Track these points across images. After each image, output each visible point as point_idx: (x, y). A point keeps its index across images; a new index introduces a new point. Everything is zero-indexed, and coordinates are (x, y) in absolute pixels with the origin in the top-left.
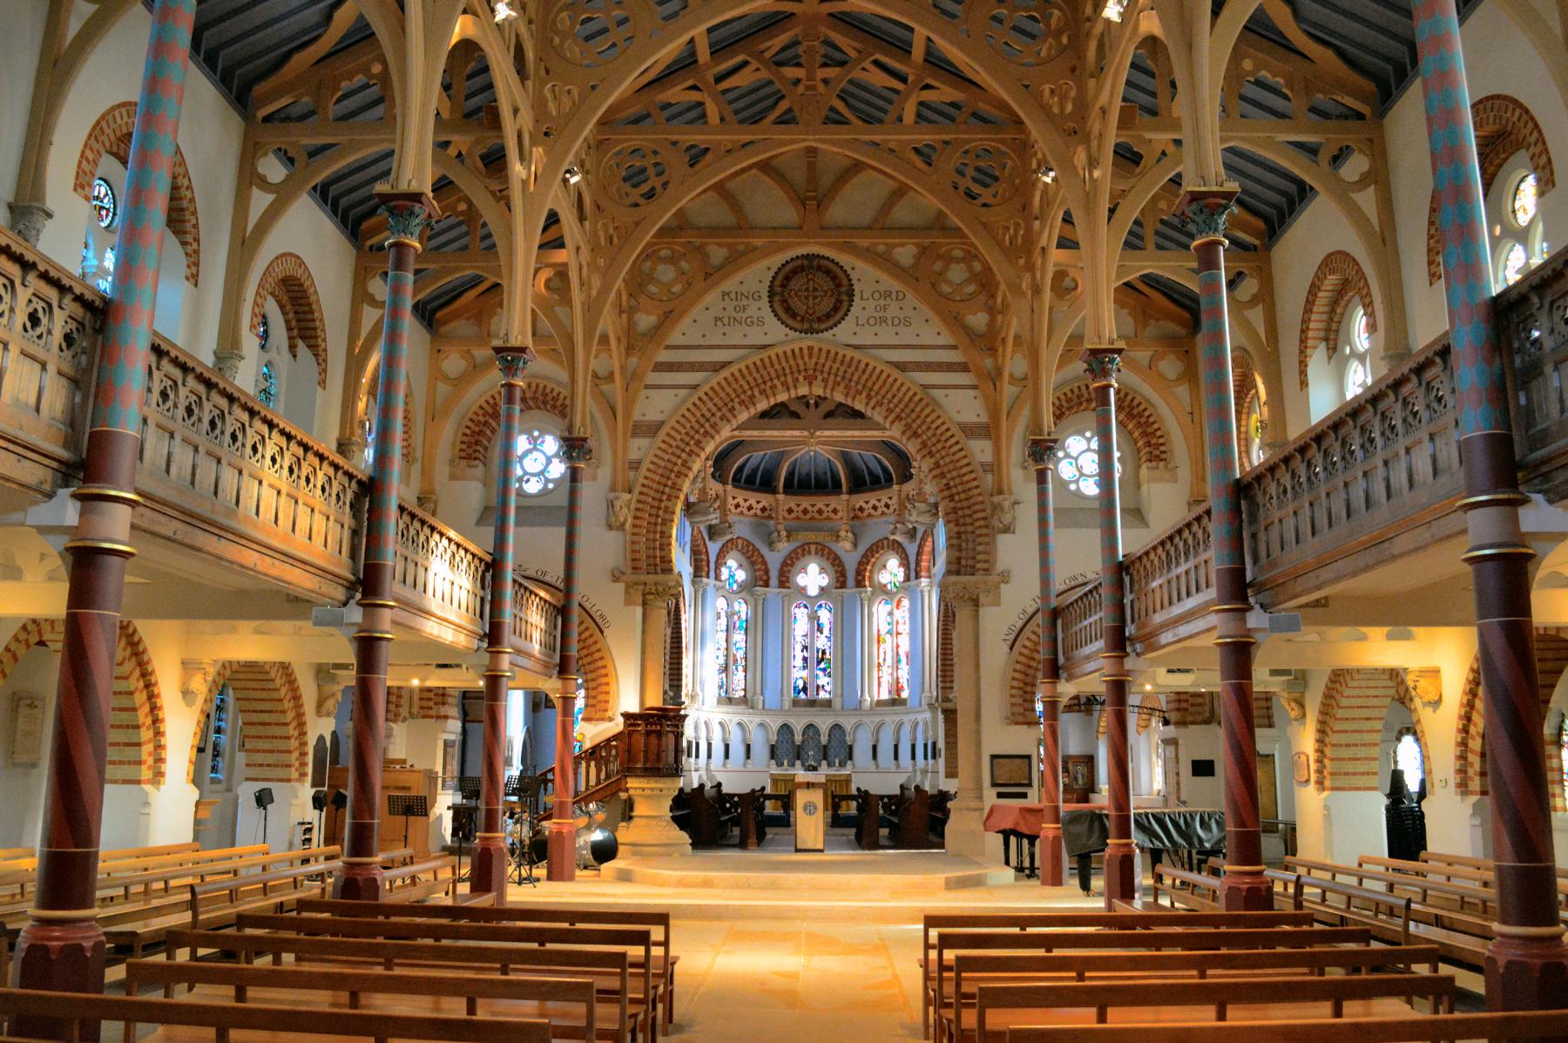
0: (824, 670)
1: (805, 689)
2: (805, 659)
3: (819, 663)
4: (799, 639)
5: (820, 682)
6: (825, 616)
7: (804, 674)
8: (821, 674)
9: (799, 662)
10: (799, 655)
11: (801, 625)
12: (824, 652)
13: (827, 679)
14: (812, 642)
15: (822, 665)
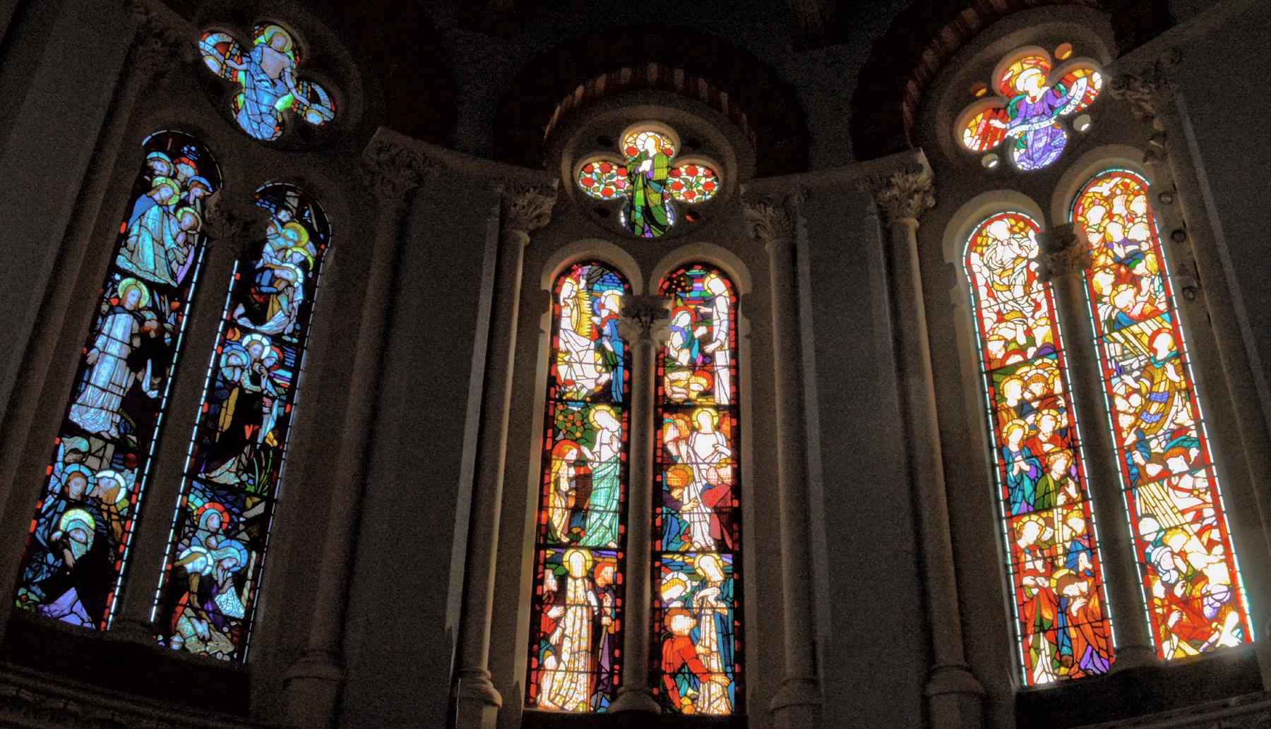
0: (230, 497)
1: (92, 576)
2: (134, 406)
3: (211, 454)
4: (134, 294)
5: (198, 561)
6: (288, 250)
7: (117, 484)
8: (213, 517)
9: (96, 412)
10: (108, 368)
11: (158, 237)
12: (250, 408)
13: (235, 554)
14: (199, 343)
15: (226, 474)
